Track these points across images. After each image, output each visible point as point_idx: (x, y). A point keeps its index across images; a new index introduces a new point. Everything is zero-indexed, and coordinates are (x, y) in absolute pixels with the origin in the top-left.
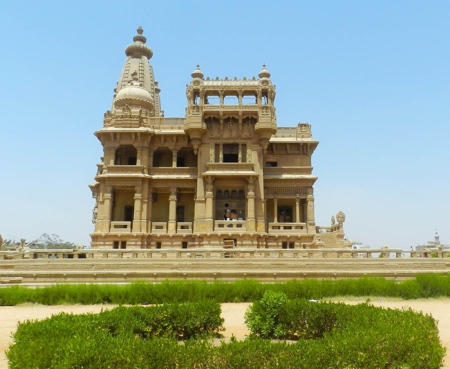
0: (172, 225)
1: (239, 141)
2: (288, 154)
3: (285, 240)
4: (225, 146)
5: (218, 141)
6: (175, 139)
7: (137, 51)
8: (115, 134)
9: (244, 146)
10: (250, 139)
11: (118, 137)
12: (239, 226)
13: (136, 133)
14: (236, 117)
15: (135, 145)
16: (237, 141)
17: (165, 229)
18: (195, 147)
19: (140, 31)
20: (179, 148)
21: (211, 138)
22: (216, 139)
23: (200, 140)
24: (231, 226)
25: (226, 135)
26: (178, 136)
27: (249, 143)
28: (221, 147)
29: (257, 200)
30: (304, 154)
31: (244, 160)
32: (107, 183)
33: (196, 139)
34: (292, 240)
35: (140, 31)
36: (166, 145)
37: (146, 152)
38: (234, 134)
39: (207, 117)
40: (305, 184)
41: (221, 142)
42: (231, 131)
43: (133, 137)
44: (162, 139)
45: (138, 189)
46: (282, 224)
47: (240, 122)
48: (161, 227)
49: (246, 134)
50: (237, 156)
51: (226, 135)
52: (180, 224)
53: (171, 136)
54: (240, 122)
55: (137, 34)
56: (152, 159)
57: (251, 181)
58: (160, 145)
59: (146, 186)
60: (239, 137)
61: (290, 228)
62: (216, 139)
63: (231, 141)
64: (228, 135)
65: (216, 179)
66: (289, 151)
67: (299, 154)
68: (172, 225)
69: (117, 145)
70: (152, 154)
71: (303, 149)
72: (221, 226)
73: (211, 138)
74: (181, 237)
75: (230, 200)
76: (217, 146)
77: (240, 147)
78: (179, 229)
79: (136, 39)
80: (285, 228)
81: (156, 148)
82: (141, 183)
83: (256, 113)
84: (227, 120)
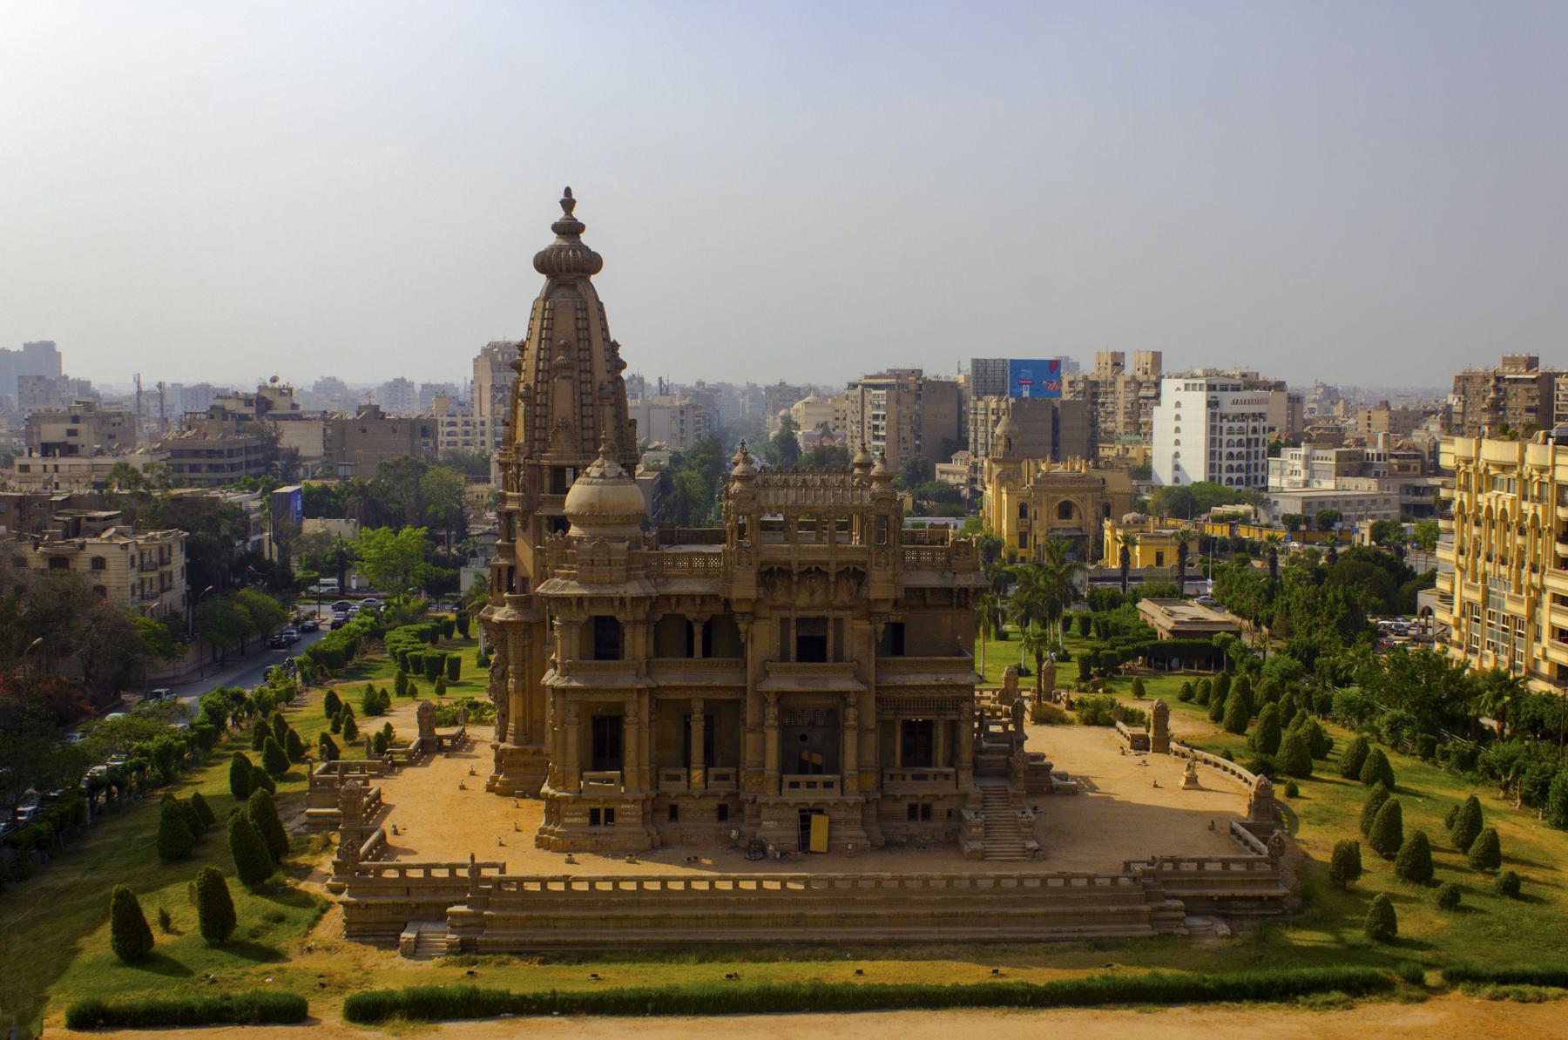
0: (697, 775)
1: (831, 614)
2: (926, 606)
3: (914, 801)
4: (799, 620)
5: (785, 614)
6: (698, 601)
7: (568, 270)
8: (580, 599)
9: (839, 621)
10: (850, 608)
11: (586, 604)
12: (828, 785)
13: (622, 599)
14: (824, 568)
15: (620, 617)
16: (824, 613)
17: (684, 782)
18: (742, 627)
19: (568, 203)
20: (706, 619)
21: (773, 608)
22: (783, 607)
23: (752, 613)
24: (811, 785)
25: (803, 599)
26: (704, 598)
27: (847, 615)
28: (793, 624)
29: (861, 730)
30: (959, 606)
31: (839, 657)
32: (569, 697)
33: (743, 614)
34: (926, 801)
35: (568, 203)
36: (680, 611)
37: (641, 630)
38: (819, 598)
39: (766, 568)
40: (956, 693)
41: (793, 615)
42: (812, 593)
43: (617, 603)
44: (673, 601)
45: (631, 709)
46: (908, 772)
47: (832, 579)
48: (677, 778)
49: (843, 597)
50: (823, 640)
51: (803, 599)
52: (712, 771)
53: (692, 597)
54: (832, 579)
55: (559, 214)
56: (651, 639)
57: (852, 700)
58: (668, 612)
59: (645, 700)
60: (829, 606)
61: (924, 777)
62: (783, 607)
63: (812, 614)
64: (805, 600)
65: (782, 696)
66: (929, 601)
67: (951, 606)
68: (697, 775)
69: (584, 617)
70: (652, 629)
71: (958, 597)
72: (794, 785)
73: (773, 608)
74: (716, 795)
75: (809, 742)
76: (785, 622)
77: (831, 624)
78: (711, 782)
79: (556, 228)
80: (915, 777)
81: (660, 617)
82: (634, 696)
83: (864, 564)
84: (803, 573)
